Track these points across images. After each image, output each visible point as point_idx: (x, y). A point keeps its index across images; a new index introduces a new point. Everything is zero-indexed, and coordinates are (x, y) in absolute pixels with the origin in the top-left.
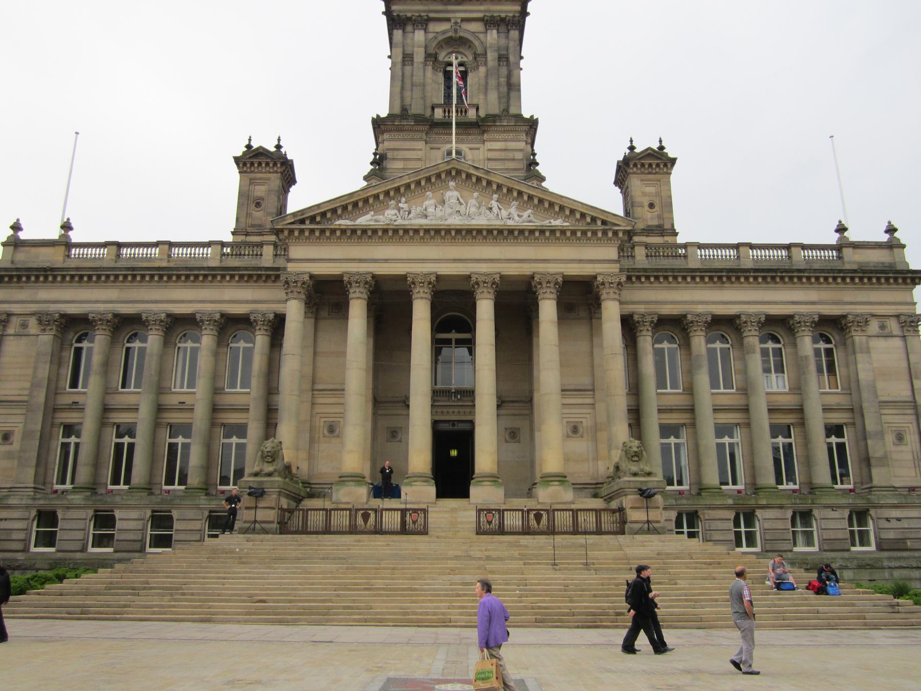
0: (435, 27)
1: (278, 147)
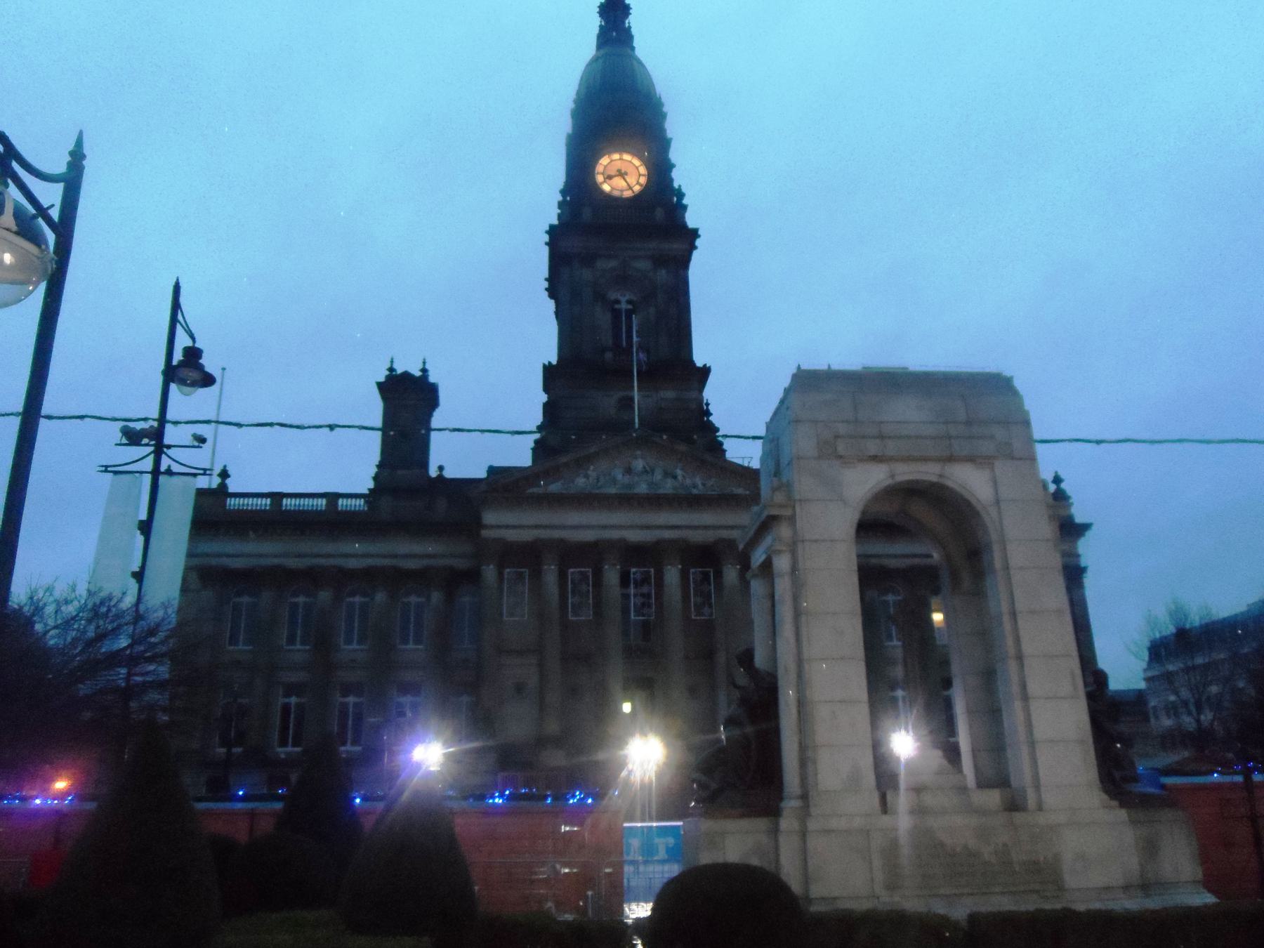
0: (602, 264)
1: (424, 371)
